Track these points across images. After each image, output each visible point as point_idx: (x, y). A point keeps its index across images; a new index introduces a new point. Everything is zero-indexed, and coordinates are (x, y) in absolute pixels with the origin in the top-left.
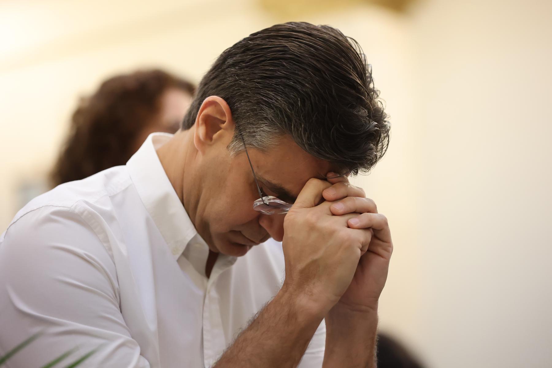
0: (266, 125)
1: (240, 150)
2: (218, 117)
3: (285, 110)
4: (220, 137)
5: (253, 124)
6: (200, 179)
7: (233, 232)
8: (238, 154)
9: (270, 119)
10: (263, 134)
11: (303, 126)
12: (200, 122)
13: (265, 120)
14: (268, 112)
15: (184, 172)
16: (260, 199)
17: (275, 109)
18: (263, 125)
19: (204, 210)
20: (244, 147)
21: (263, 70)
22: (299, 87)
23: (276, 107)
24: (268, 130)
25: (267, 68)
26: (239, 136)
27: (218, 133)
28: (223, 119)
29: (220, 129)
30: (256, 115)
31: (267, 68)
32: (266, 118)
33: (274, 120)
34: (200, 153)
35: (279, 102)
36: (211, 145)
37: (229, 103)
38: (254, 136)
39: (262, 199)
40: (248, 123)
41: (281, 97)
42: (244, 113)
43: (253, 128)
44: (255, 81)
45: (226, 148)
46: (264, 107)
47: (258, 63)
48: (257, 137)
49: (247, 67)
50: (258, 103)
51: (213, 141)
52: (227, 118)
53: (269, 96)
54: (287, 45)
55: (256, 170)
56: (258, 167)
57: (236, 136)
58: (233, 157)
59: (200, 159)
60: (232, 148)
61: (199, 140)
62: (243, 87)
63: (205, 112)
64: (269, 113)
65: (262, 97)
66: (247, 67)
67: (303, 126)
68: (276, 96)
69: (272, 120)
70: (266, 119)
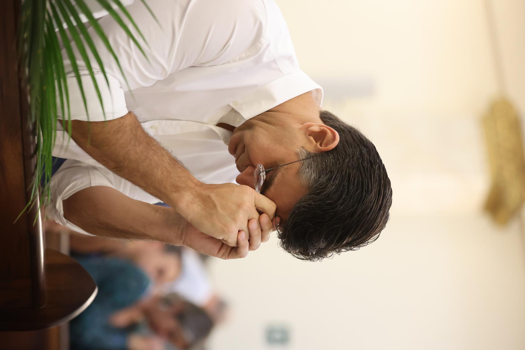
0: (315, 177)
1: (299, 156)
2: (325, 141)
3: (324, 191)
4: (310, 142)
5: (317, 167)
6: (283, 126)
7: (244, 147)
8: (297, 154)
9: (319, 180)
10: (309, 174)
11: (313, 203)
12: (322, 128)
13: (319, 176)
14: (324, 179)
15: (289, 113)
16: (264, 170)
17: (326, 184)
18: (315, 174)
19: (261, 127)
20: (301, 159)
21: (355, 176)
22: (341, 201)
23: (327, 185)
24: (312, 178)
25: (356, 180)
26: (310, 156)
27: (314, 140)
28: (323, 145)
29: (316, 142)
30: (323, 170)
31: (356, 180)
32: (320, 177)
33: (319, 183)
34: (300, 126)
35: (331, 187)
36: (305, 134)
37: (333, 150)
38: (308, 167)
39: (264, 171)
40: (318, 163)
41: (334, 189)
42: (325, 161)
43: (314, 167)
44: (348, 170)
45: (302, 145)
46: (328, 176)
47: (360, 172)
48: (308, 169)
49: (359, 164)
50: (331, 172)
51: (308, 136)
52: (323, 148)
53: (335, 179)
54: (372, 194)
55: (285, 167)
56: (287, 168)
57: (310, 154)
58: (295, 150)
59: (296, 126)
60: (301, 150)
61: (309, 126)
62: (344, 161)
63: (329, 132)
64: (324, 179)
65: (335, 175)
66: (359, 164)
67: (313, 203)
68: (335, 185)
69: (318, 182)
70: (319, 177)
